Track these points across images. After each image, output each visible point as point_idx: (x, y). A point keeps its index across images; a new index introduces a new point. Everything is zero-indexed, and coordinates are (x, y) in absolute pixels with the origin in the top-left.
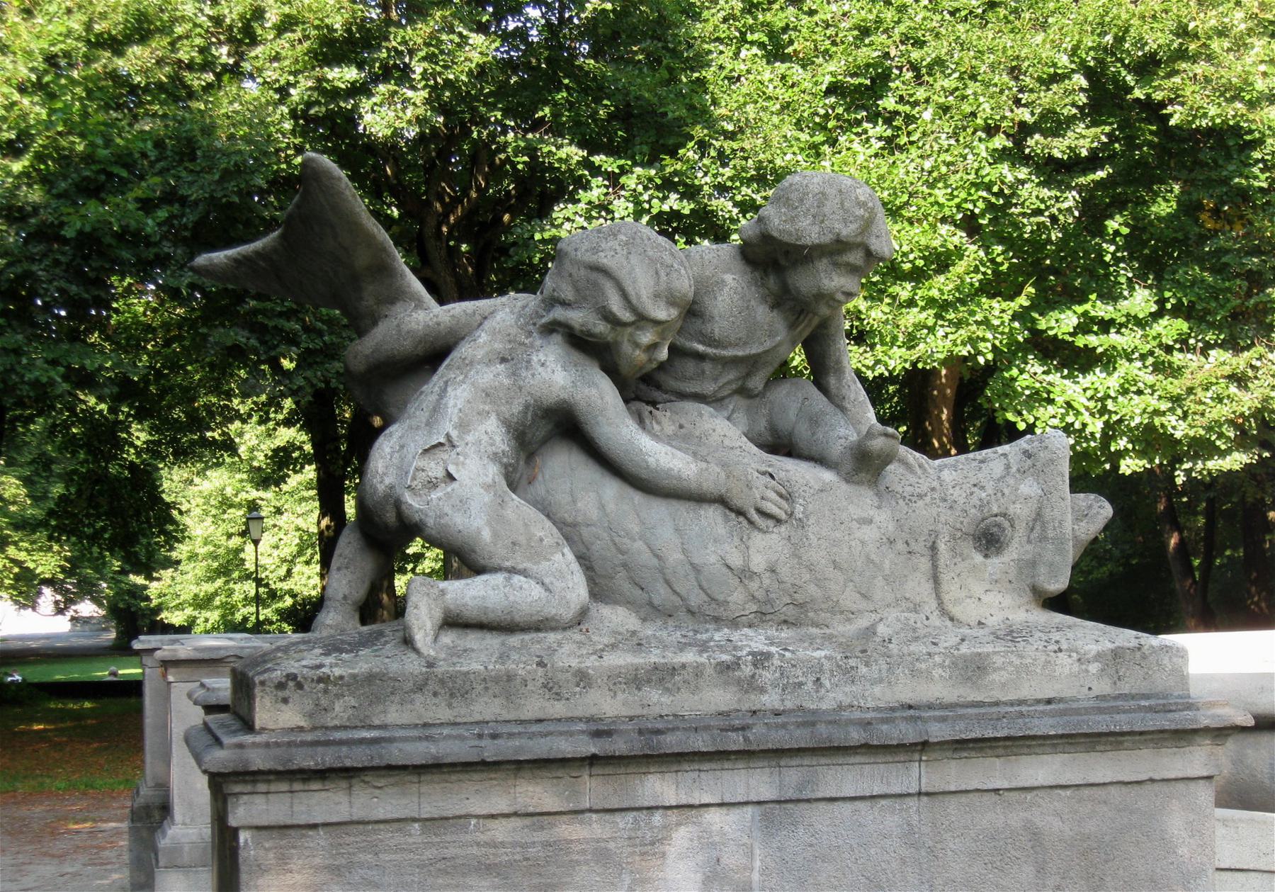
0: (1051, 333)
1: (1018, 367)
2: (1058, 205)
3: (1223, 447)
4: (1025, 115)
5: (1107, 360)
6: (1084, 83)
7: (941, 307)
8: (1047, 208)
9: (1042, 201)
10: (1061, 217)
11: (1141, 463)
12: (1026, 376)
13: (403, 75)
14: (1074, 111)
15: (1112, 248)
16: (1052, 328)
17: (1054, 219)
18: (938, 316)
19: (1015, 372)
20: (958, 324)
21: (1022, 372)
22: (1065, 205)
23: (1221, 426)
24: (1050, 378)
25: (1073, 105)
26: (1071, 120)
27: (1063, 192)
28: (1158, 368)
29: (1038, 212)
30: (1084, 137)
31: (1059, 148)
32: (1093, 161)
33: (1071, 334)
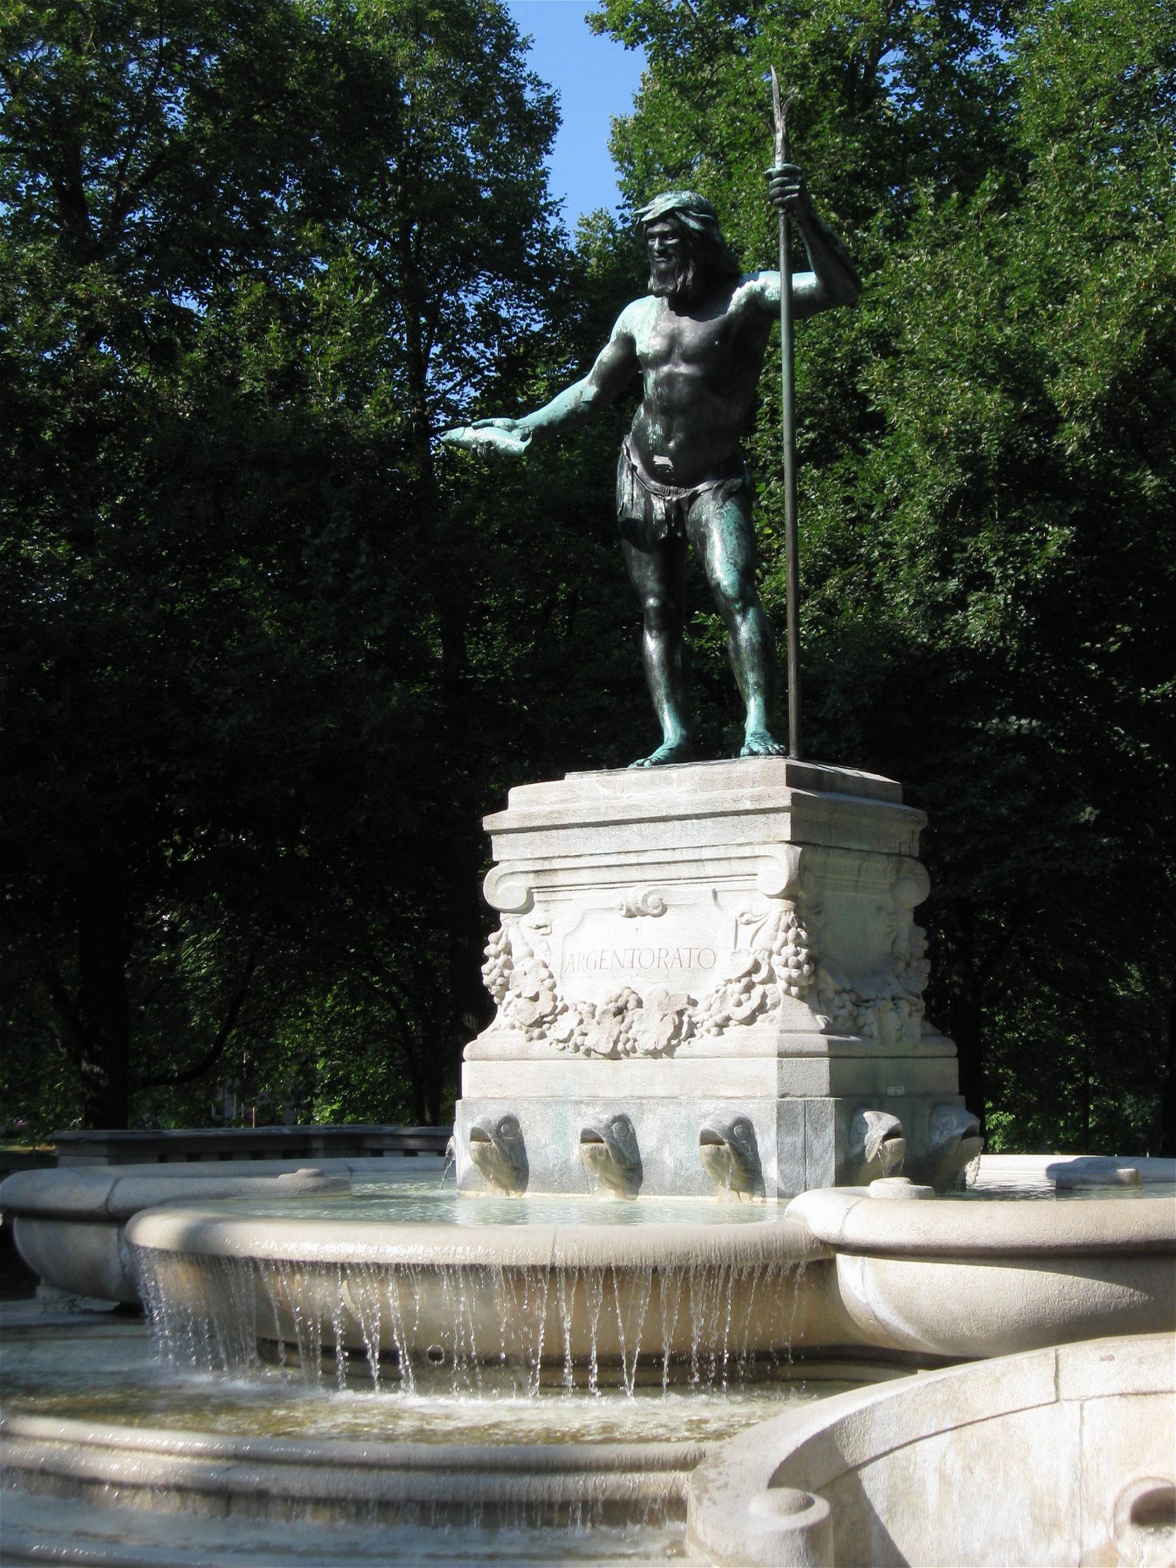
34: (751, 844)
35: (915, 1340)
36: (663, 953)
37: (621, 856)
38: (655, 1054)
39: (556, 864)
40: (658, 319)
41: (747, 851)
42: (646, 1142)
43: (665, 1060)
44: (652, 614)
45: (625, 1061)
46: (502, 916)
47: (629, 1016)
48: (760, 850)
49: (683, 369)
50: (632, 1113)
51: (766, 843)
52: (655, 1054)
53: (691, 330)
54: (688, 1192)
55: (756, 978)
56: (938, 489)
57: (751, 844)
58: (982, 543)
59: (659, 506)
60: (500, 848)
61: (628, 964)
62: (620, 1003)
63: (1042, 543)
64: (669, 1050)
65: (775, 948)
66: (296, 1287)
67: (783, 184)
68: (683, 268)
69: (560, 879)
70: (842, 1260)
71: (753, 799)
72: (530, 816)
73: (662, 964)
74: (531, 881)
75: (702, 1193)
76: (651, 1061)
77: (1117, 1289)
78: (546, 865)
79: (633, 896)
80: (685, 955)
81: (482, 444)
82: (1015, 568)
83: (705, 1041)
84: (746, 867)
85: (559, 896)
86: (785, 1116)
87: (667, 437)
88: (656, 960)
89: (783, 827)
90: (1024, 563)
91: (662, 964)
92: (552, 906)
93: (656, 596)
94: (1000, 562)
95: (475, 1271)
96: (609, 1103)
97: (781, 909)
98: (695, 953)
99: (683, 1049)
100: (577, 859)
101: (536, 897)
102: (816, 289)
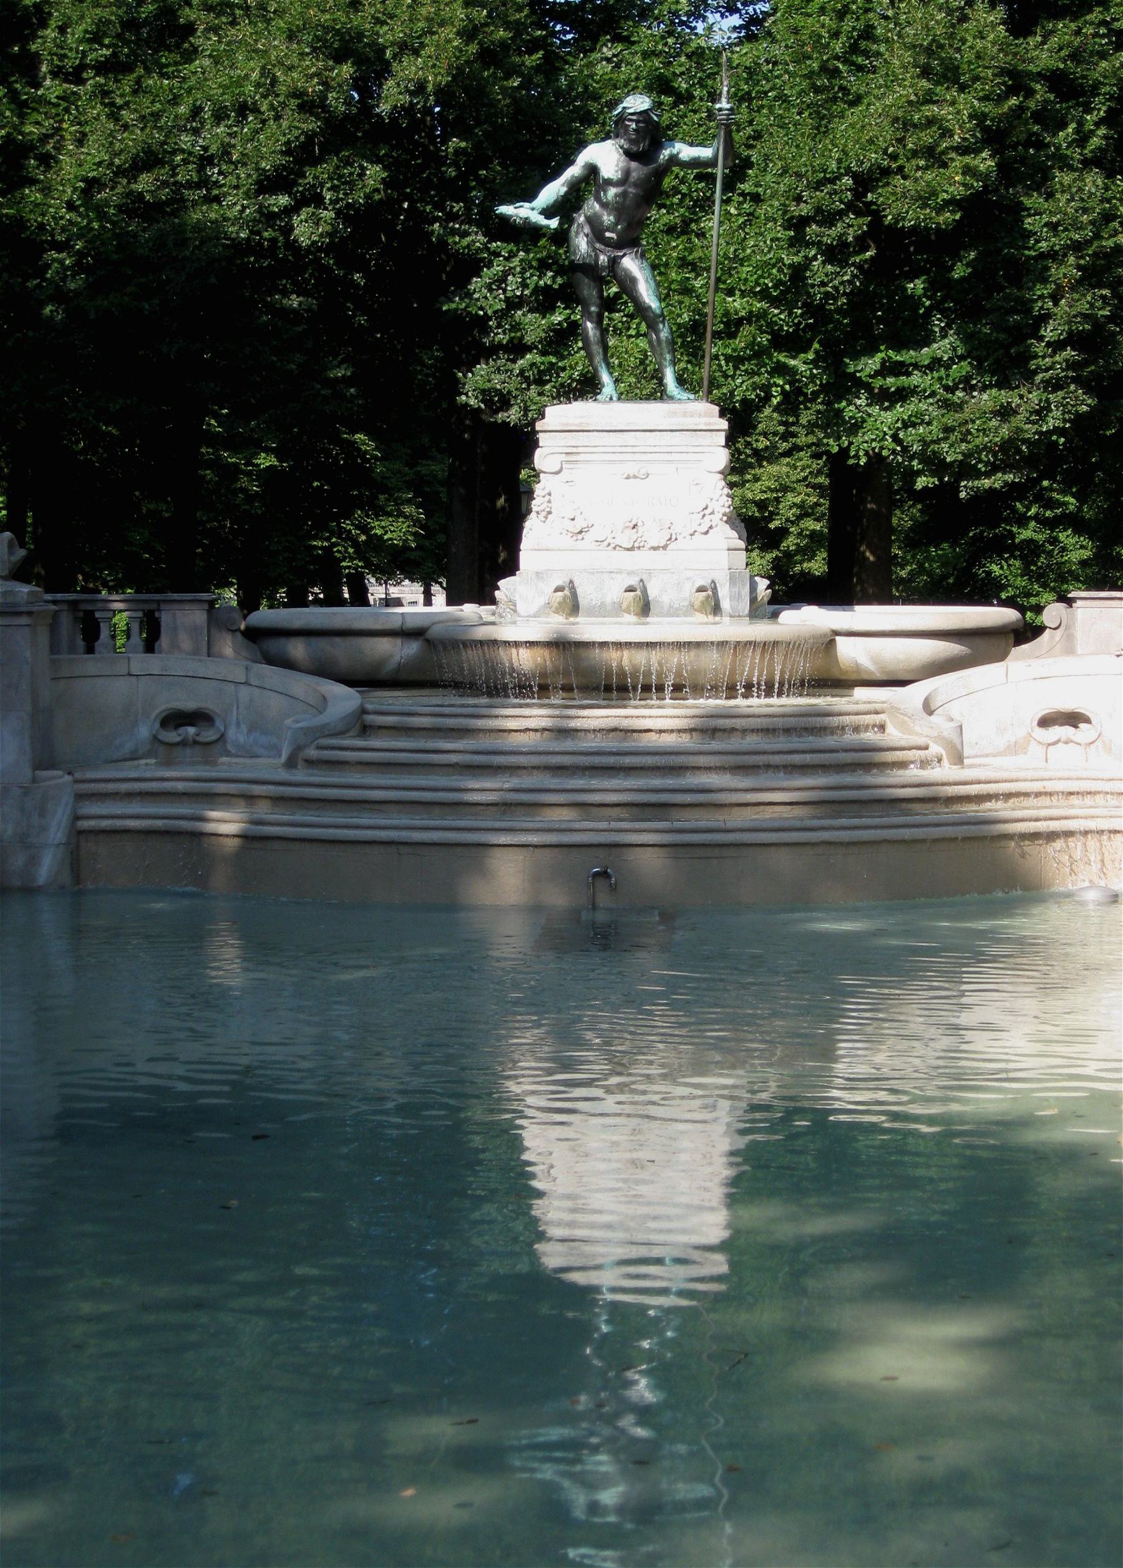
0: (858, 375)
1: (847, 400)
2: (839, 278)
3: (983, 469)
4: (805, 210)
5: (903, 395)
6: (851, 182)
7: (736, 360)
8: (831, 280)
9: (827, 275)
10: (841, 288)
11: (932, 480)
12: (852, 408)
13: (317, 200)
14: (842, 206)
15: (928, 303)
16: (859, 371)
17: (836, 288)
18: (736, 368)
19: (844, 404)
20: (753, 374)
21: (850, 403)
22: (846, 278)
23: (979, 453)
24: (870, 410)
25: (841, 202)
26: (841, 213)
27: (842, 268)
28: (946, 405)
29: (823, 284)
30: (852, 226)
31: (830, 235)
32: (861, 243)
33: (871, 376)
35: (873, 672)
38: (655, 548)
40: (619, 160)
42: (652, 594)
43: (661, 551)
44: (594, 315)
45: (636, 552)
46: (542, 475)
47: (640, 529)
49: (632, 190)
50: (645, 578)
52: (655, 548)
53: (638, 170)
54: (678, 616)
55: (707, 512)
56: (296, 133)
58: (323, 171)
59: (603, 259)
60: (542, 438)
62: (634, 522)
63: (362, 175)
64: (665, 547)
65: (715, 498)
66: (613, 657)
67: (728, 115)
68: (644, 139)
70: (838, 638)
71: (706, 424)
72: (567, 424)
74: (564, 457)
75: (685, 616)
76: (652, 552)
77: (963, 648)
78: (574, 450)
79: (631, 468)
82: (346, 194)
83: (681, 543)
86: (733, 579)
87: (617, 224)
89: (721, 439)
90: (351, 190)
93: (597, 306)
94: (333, 188)
95: (722, 644)
96: (631, 573)
99: (672, 546)
101: (564, 466)
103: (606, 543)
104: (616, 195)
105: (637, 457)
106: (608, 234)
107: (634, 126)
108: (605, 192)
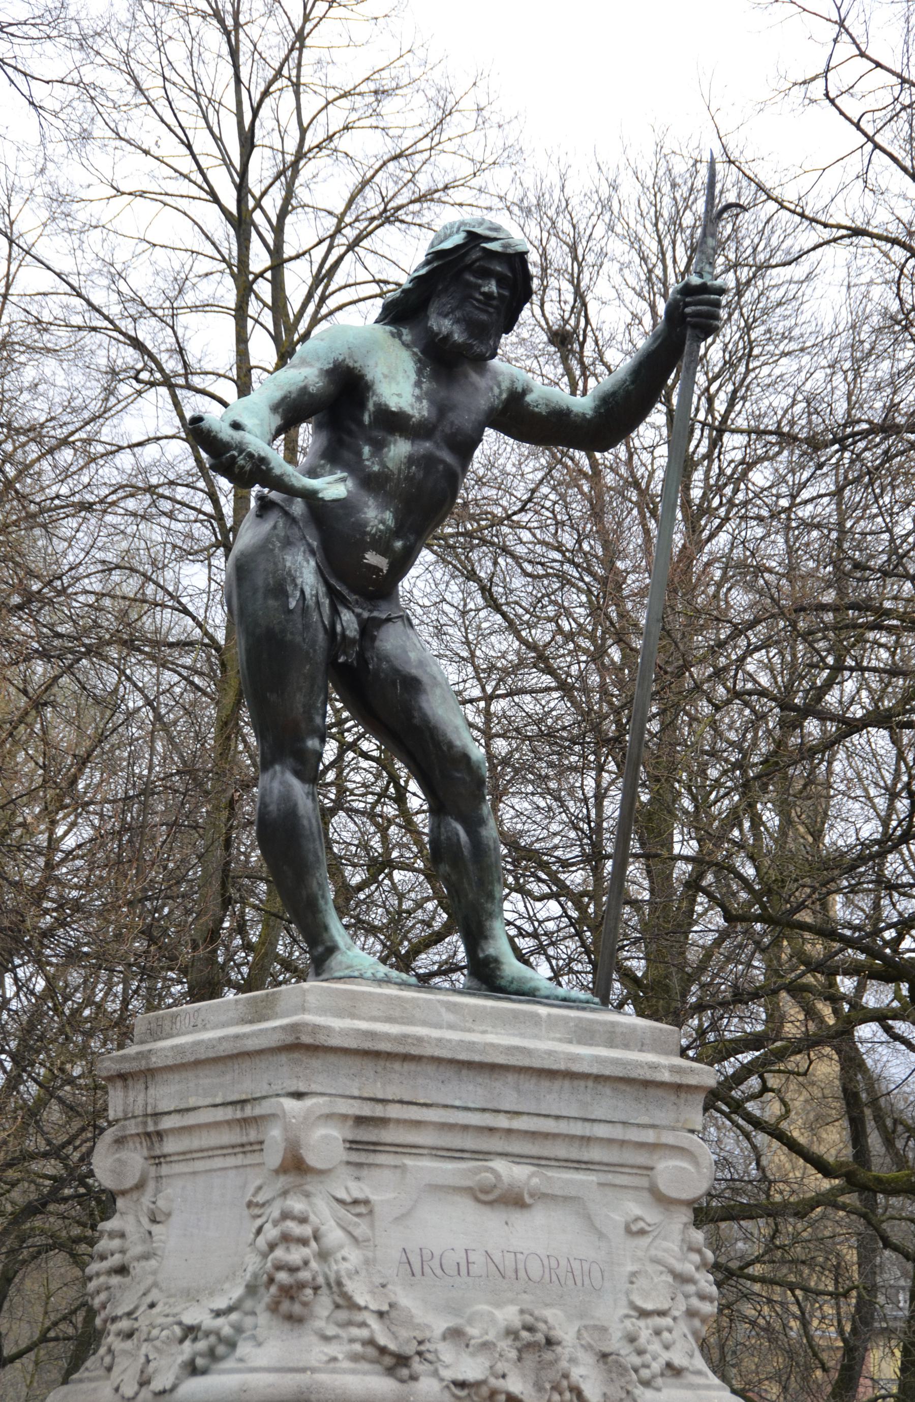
34: (653, 1126)
36: (554, 1264)
37: (487, 1115)
39: (394, 1112)
40: (419, 372)
41: (649, 1136)
48: (668, 1138)
51: (674, 1129)
57: (653, 1126)
61: (510, 1273)
69: (388, 1135)
71: (673, 1069)
73: (554, 1278)
78: (378, 1111)
80: (576, 1265)
81: (250, 456)
84: (641, 1158)
85: (381, 1159)
88: (547, 1271)
91: (554, 1278)
92: (365, 1172)
97: (685, 1219)
98: (586, 1266)
100: (424, 1110)
102: (590, 421)
103: (485, 1391)
104: (411, 460)
105: (517, 1147)
106: (372, 558)
107: (492, 287)
108: (379, 446)
